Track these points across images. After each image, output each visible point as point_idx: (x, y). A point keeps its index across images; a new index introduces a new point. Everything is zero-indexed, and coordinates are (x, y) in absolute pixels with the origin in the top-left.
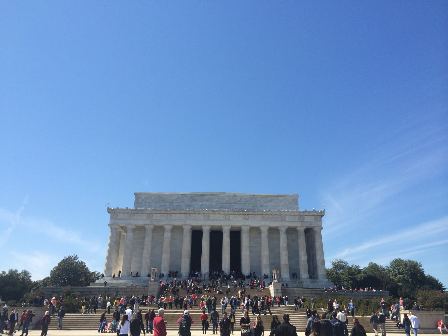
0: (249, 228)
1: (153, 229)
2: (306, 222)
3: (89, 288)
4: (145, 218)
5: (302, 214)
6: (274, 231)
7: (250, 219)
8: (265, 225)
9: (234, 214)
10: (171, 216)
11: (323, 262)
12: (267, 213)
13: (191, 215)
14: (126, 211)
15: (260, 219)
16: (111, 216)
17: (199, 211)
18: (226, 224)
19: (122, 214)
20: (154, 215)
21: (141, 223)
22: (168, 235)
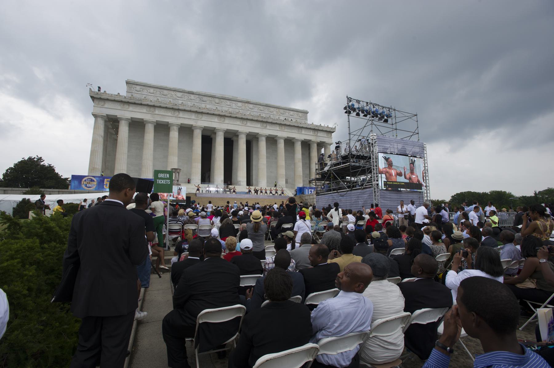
5: (317, 128)
6: (290, 143)
7: (268, 127)
9: (252, 120)
13: (204, 115)
14: (117, 99)
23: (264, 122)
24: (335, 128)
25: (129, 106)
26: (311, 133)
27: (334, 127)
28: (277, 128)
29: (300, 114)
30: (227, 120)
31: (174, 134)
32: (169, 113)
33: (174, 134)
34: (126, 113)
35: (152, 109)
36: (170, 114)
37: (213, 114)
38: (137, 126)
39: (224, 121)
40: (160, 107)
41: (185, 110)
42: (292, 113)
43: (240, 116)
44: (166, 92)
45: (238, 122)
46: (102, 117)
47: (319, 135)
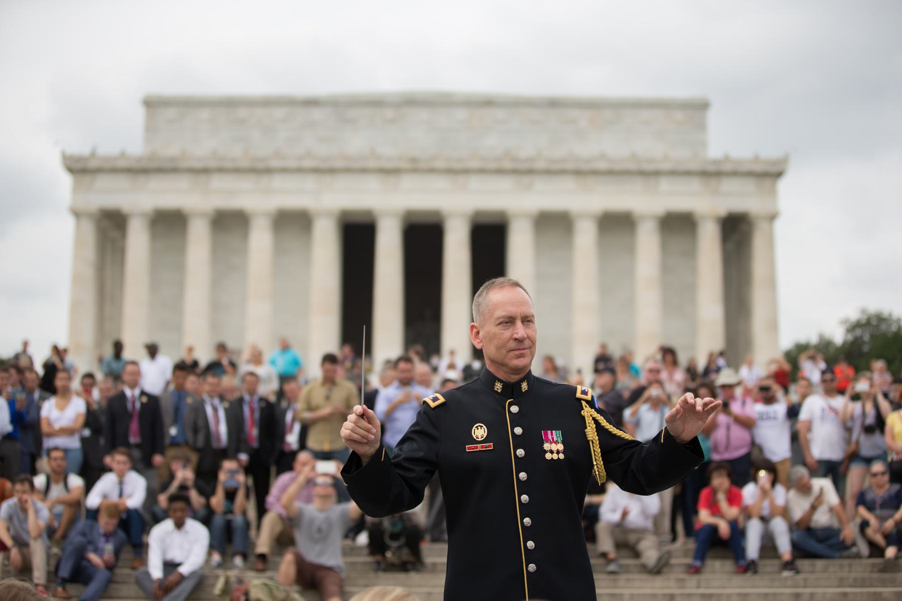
6: (616, 225)
11: (773, 326)
23: (523, 172)
24: (785, 160)
26: (695, 184)
28: (569, 183)
29: (679, 115)
30: (408, 182)
31: (261, 238)
32: (245, 183)
33: (261, 238)
34: (140, 199)
38: (169, 224)
42: (646, 114)
44: (243, 112)
45: (441, 183)
46: (90, 215)
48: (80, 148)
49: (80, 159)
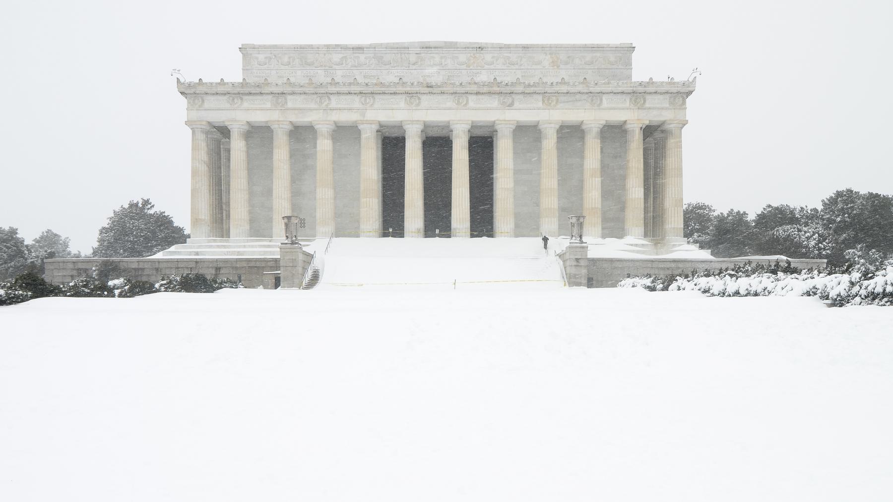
0: (514, 127)
1: (291, 131)
2: (650, 108)
3: (153, 261)
4: (268, 105)
5: (641, 89)
6: (571, 133)
7: (517, 104)
8: (551, 117)
9: (477, 93)
10: (329, 99)
12: (557, 88)
13: (377, 97)
14: (221, 89)
15: (540, 104)
16: (189, 103)
17: (396, 84)
18: (460, 120)
19: (212, 98)
20: (289, 97)
21: (259, 117)
22: (324, 145)
25: (242, 99)
27: (691, 80)
35: (281, 99)
36: (313, 105)
37: (395, 93)
39: (418, 105)
40: (293, 93)
41: (338, 93)
43: (450, 89)
47: (647, 105)
48: (191, 77)
49: (190, 85)
